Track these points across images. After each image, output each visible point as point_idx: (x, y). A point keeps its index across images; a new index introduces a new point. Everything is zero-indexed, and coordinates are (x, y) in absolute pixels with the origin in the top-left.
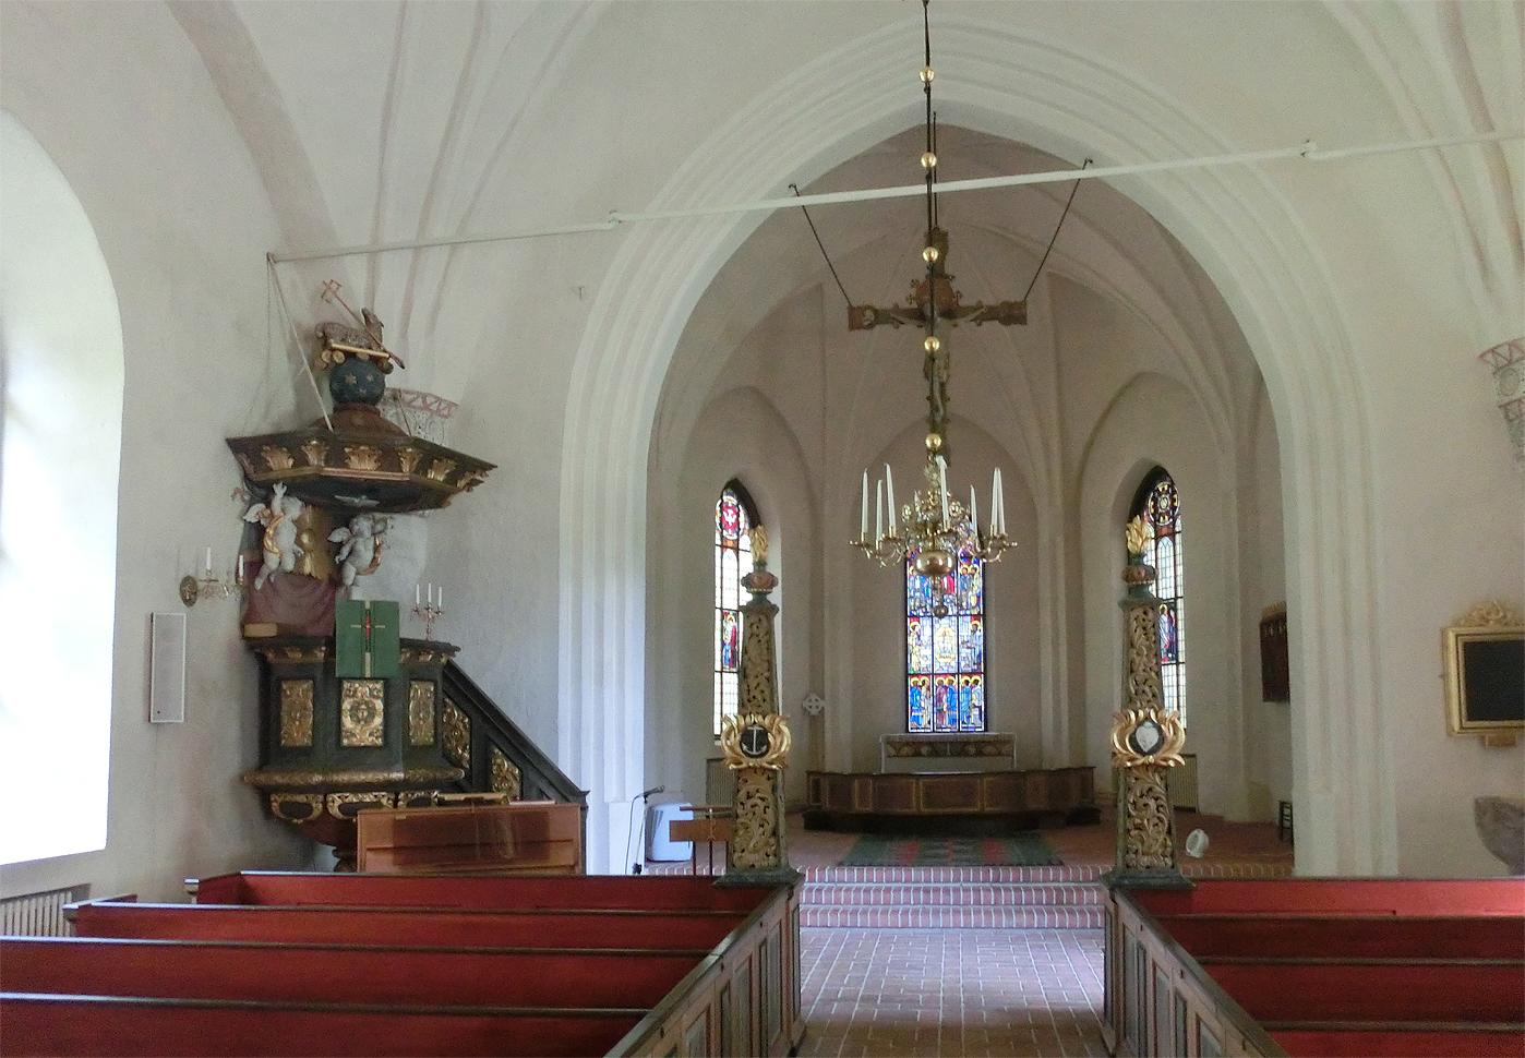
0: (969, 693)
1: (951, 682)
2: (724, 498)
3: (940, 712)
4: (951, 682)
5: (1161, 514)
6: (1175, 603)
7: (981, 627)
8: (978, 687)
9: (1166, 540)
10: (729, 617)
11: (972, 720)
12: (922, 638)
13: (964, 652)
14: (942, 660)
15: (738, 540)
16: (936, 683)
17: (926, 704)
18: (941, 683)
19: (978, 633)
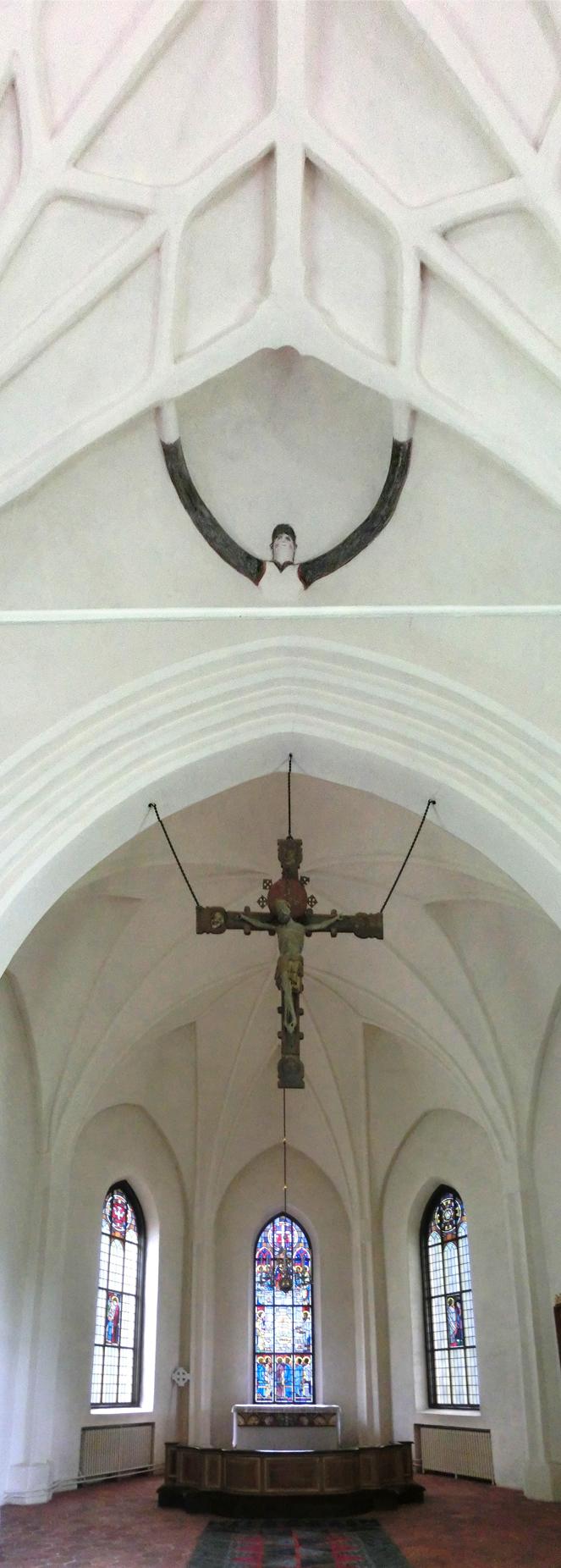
0: (301, 1370)
1: (288, 1361)
2: (115, 1196)
3: (280, 1385)
4: (288, 1361)
5: (446, 1224)
6: (461, 1296)
7: (310, 1316)
9: (451, 1245)
10: (113, 1297)
11: (304, 1393)
13: (298, 1335)
14: (281, 1342)
15: (125, 1233)
16: (276, 1361)
17: (269, 1378)
18: (280, 1361)
19: (308, 1320)
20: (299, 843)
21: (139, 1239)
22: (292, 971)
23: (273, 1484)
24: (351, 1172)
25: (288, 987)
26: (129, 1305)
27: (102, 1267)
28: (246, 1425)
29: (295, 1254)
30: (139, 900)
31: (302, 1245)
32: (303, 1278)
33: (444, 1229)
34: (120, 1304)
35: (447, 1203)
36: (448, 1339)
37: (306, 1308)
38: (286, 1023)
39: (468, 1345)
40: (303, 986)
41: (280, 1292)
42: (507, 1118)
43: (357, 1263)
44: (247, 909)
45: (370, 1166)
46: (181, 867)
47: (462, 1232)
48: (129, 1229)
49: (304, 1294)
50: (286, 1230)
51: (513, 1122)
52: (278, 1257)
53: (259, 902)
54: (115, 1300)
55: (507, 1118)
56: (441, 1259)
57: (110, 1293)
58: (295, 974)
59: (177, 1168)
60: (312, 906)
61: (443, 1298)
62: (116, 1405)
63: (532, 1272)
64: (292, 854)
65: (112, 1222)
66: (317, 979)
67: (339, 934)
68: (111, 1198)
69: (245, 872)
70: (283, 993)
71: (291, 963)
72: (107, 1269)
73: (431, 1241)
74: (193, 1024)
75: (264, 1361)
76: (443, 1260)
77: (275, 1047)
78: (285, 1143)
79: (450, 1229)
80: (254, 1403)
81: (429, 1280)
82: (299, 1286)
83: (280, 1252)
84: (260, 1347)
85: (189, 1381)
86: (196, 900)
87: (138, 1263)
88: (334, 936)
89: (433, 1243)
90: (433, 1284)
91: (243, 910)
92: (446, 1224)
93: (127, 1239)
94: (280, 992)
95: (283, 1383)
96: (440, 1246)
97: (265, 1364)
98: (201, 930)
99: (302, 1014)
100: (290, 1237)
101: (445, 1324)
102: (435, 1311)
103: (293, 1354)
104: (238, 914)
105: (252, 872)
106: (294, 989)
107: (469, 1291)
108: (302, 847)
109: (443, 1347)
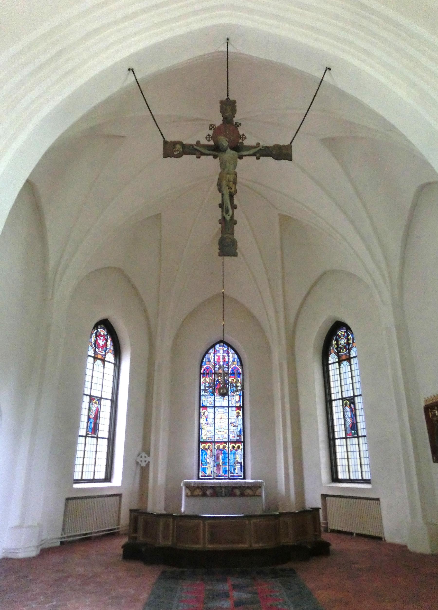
0: (234, 454)
1: (224, 447)
3: (218, 466)
4: (224, 447)
5: (341, 348)
6: (354, 399)
7: (241, 414)
8: (240, 450)
9: (345, 363)
10: (94, 401)
11: (236, 471)
12: (208, 419)
13: (232, 428)
15: (105, 355)
16: (216, 447)
17: (210, 460)
18: (218, 447)
20: (234, 102)
21: (115, 359)
22: (229, 181)
23: (212, 541)
24: (271, 312)
25: (226, 191)
26: (106, 407)
27: (87, 380)
28: (192, 496)
29: (230, 369)
30: (124, 137)
31: (235, 363)
32: (236, 387)
33: (340, 352)
34: (99, 406)
35: (341, 334)
37: (238, 408)
38: (224, 214)
39: (360, 435)
40: (236, 190)
41: (219, 397)
42: (383, 276)
43: (276, 375)
44: (198, 142)
45: (285, 309)
46: (153, 117)
47: (353, 354)
48: (108, 352)
49: (237, 398)
50: (223, 353)
51: (387, 278)
52: (217, 372)
53: (206, 138)
54: (96, 403)
55: (383, 276)
56: (338, 373)
57: (92, 398)
58: (231, 183)
59: (145, 310)
60: (243, 140)
61: (341, 401)
62: (93, 481)
63: (406, 383)
64: (229, 109)
65: (96, 347)
66: (246, 186)
67: (262, 158)
68: (96, 331)
69: (197, 119)
70: (223, 195)
71: (228, 176)
72: (90, 381)
73: (331, 360)
74: (159, 216)
75: (207, 447)
76: (340, 374)
77: (217, 230)
78: (223, 293)
79: (344, 352)
80: (199, 478)
81: (330, 388)
82: (233, 392)
83: (219, 368)
84: (204, 437)
85: (149, 462)
86: (163, 137)
87: (114, 376)
88: (258, 158)
89: (332, 362)
90: (333, 390)
91: (195, 143)
92: (341, 348)
93: (106, 359)
94: (220, 194)
95: (221, 464)
96: (337, 364)
97: (207, 449)
98: (166, 155)
99: (236, 208)
100: (226, 357)
101: (343, 420)
102: (335, 410)
103: (229, 442)
104: (192, 146)
105: (202, 120)
106: (230, 192)
107: (360, 395)
108: (236, 104)
109: (341, 437)
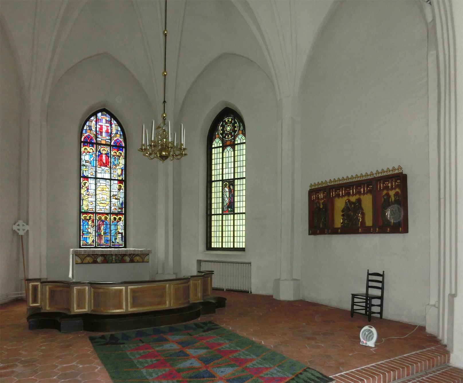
5: (226, 134)
33: (225, 137)
36: (223, 208)
39: (236, 212)
61: (221, 182)
92: (226, 134)
96: (221, 149)
